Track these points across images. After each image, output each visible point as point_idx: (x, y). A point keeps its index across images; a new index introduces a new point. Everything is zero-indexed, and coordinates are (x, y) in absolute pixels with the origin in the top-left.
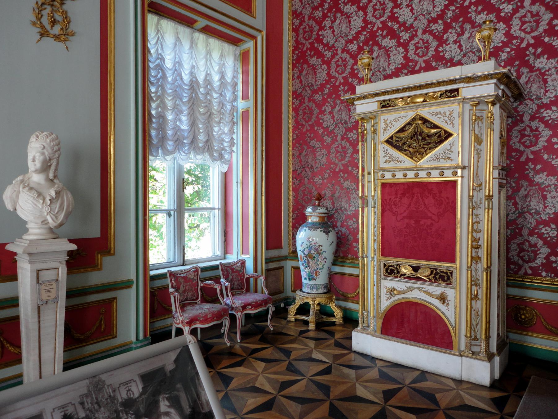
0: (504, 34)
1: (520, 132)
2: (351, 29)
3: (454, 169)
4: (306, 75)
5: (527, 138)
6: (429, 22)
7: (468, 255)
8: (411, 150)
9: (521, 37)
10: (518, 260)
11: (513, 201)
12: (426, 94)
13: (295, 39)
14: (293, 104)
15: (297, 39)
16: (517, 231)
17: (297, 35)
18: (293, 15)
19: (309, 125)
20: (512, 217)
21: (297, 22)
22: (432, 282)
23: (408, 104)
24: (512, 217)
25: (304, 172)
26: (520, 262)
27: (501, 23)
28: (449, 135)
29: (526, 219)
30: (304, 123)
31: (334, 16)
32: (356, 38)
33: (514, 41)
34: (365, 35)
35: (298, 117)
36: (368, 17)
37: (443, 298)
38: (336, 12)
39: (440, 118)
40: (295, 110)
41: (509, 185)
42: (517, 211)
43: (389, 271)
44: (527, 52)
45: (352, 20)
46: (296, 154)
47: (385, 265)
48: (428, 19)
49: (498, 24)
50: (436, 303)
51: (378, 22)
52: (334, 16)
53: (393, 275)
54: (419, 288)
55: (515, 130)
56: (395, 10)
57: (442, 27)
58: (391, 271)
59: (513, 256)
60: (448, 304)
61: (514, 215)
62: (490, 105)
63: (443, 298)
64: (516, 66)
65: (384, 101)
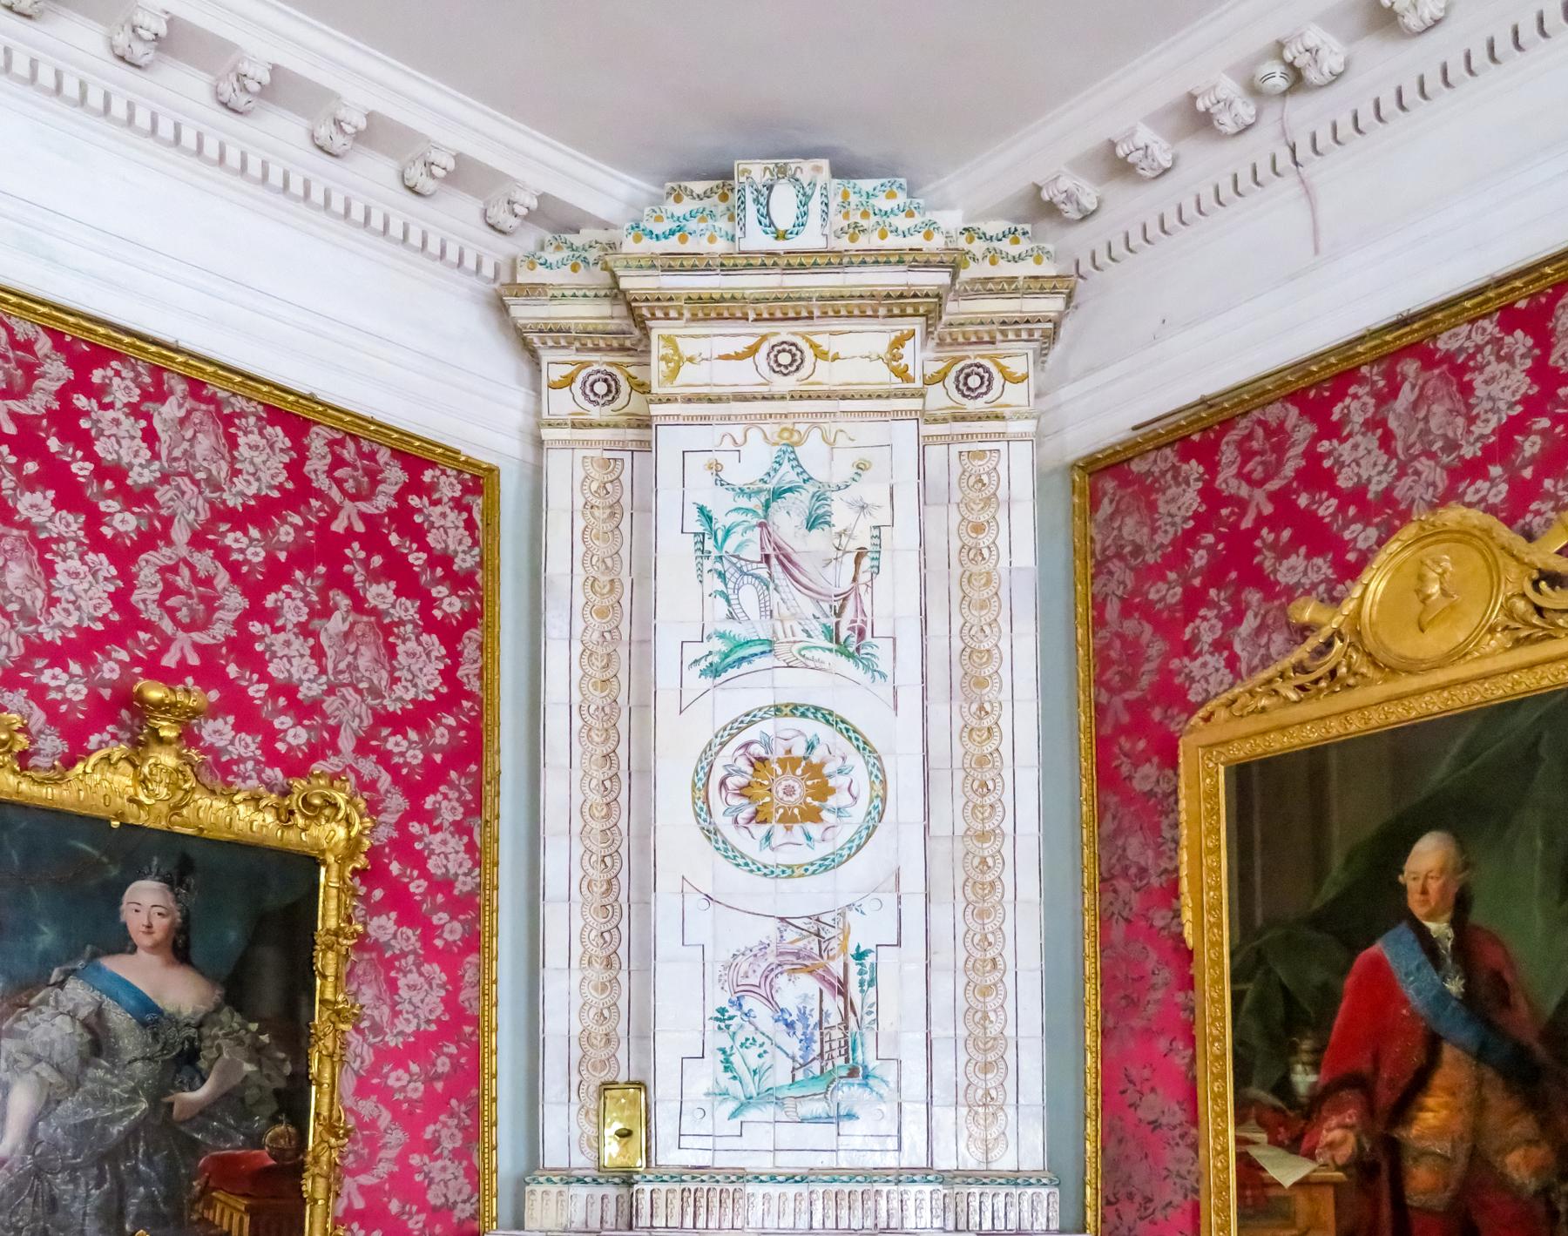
36: (1221, 477)
51: (1259, 495)
56: (1324, 446)
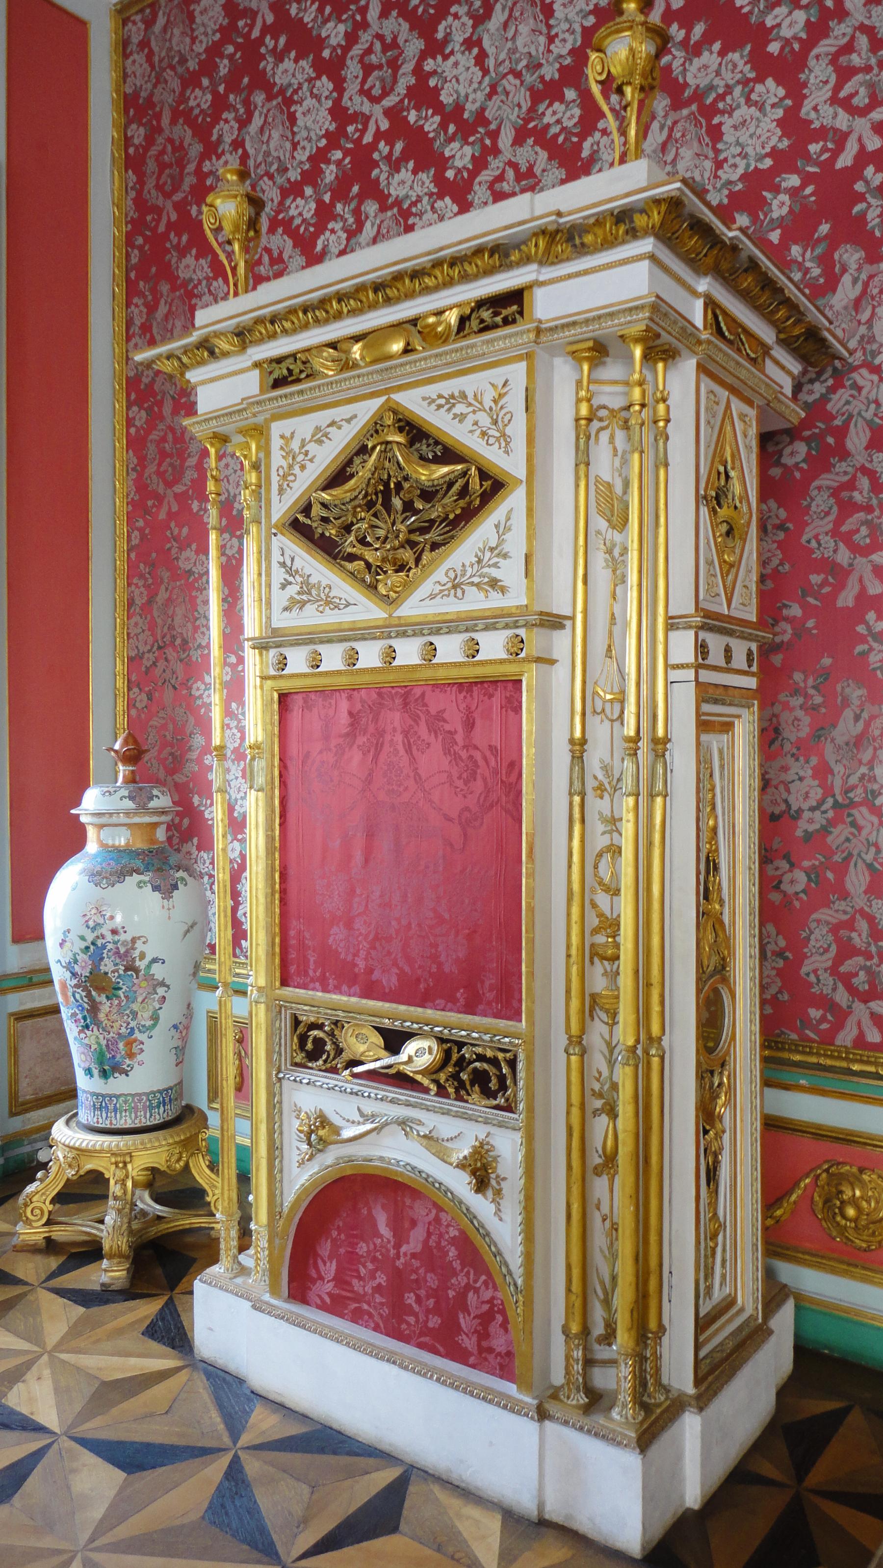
0: (780, 123)
1: (835, 493)
2: (295, 146)
3: (507, 626)
4: (166, 317)
5: (861, 515)
6: (537, 97)
7: (568, 991)
8: (369, 556)
9: (836, 130)
10: (834, 989)
11: (814, 761)
12: (414, 322)
13: (133, 194)
14: (129, 422)
15: (139, 193)
16: (830, 875)
17: (141, 182)
18: (126, 112)
19: (176, 496)
20: (811, 821)
21: (138, 134)
22: (447, 1096)
23: (355, 366)
24: (811, 821)
25: (161, 664)
26: (842, 997)
27: (770, 82)
28: (494, 486)
29: (860, 829)
30: (161, 489)
31: (247, 103)
32: (311, 176)
33: (814, 148)
34: (339, 163)
35: (144, 467)
36: (346, 96)
37: (481, 1170)
38: (251, 88)
39: (462, 418)
40: (135, 444)
41: (801, 700)
42: (830, 801)
43: (309, 1046)
44: (859, 187)
45: (299, 110)
46: (139, 602)
47: (296, 1022)
48: (531, 89)
49: (759, 88)
50: (460, 1183)
51: (377, 111)
52: (247, 103)
53: (320, 1062)
54: (403, 1123)
55: (819, 488)
56: (429, 65)
57: (577, 112)
58: (314, 1046)
59: (815, 971)
60: (498, 1192)
61: (817, 813)
62: (638, 352)
63: (481, 1170)
64: (819, 240)
65: (279, 360)
